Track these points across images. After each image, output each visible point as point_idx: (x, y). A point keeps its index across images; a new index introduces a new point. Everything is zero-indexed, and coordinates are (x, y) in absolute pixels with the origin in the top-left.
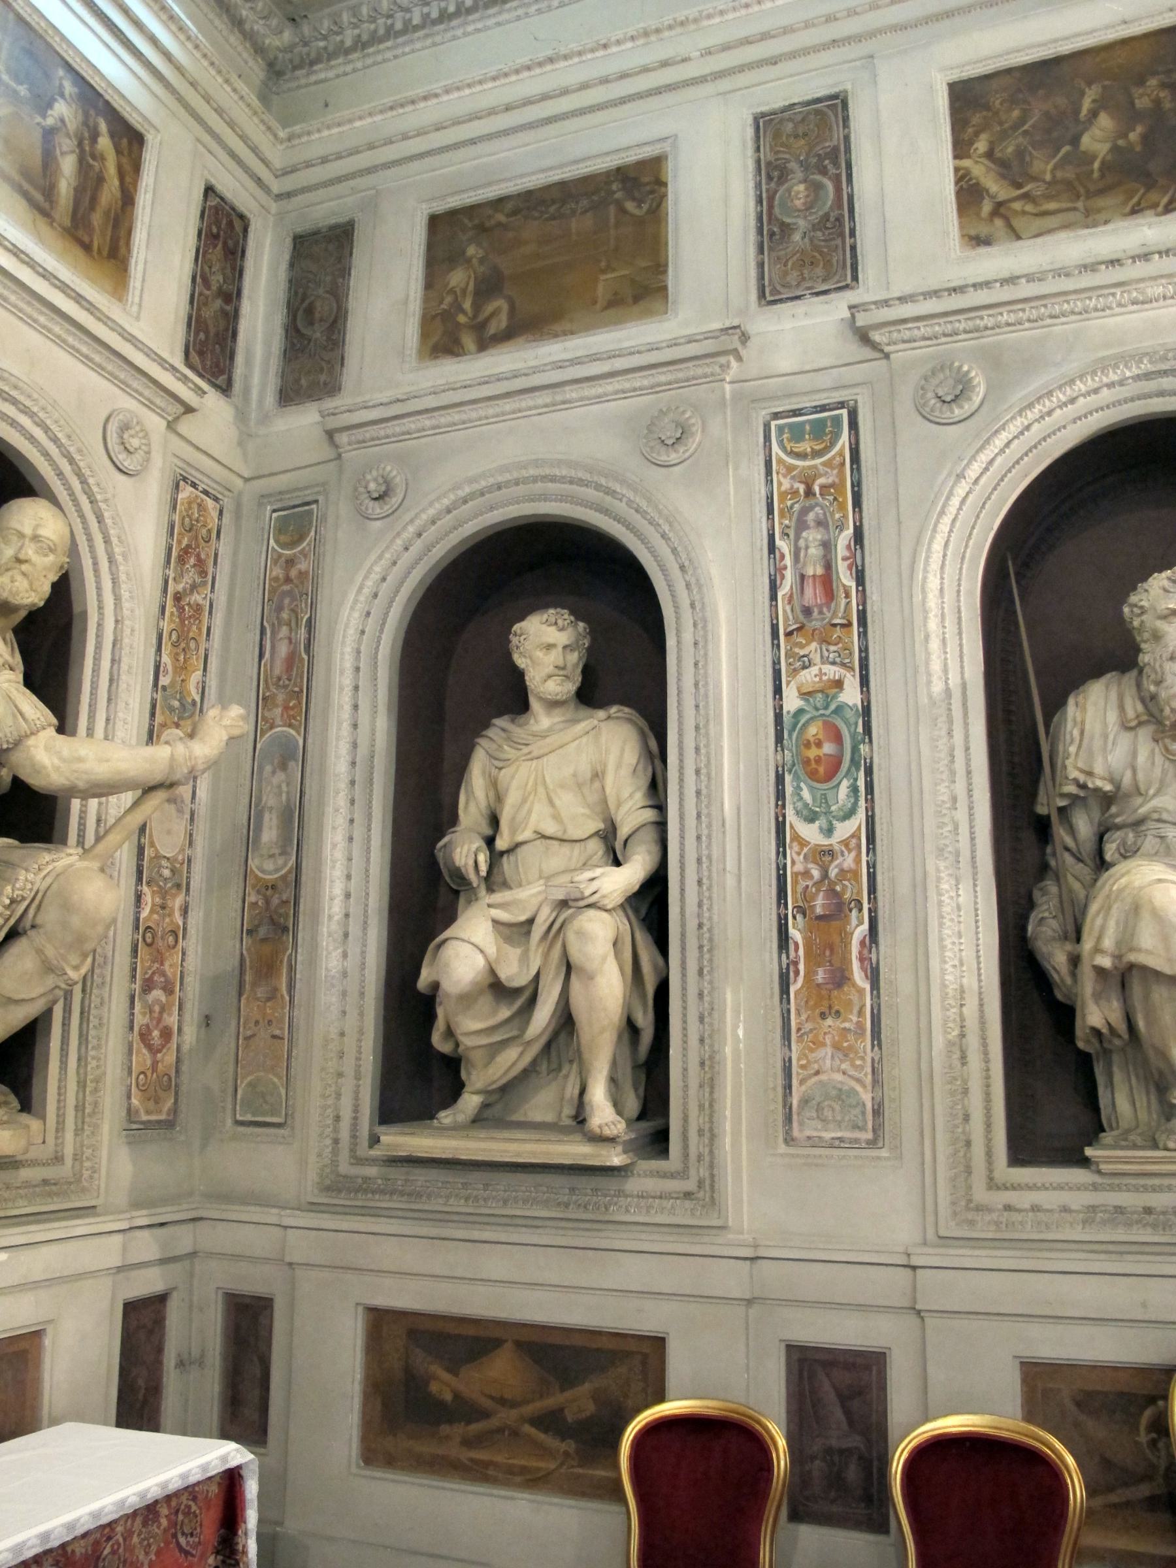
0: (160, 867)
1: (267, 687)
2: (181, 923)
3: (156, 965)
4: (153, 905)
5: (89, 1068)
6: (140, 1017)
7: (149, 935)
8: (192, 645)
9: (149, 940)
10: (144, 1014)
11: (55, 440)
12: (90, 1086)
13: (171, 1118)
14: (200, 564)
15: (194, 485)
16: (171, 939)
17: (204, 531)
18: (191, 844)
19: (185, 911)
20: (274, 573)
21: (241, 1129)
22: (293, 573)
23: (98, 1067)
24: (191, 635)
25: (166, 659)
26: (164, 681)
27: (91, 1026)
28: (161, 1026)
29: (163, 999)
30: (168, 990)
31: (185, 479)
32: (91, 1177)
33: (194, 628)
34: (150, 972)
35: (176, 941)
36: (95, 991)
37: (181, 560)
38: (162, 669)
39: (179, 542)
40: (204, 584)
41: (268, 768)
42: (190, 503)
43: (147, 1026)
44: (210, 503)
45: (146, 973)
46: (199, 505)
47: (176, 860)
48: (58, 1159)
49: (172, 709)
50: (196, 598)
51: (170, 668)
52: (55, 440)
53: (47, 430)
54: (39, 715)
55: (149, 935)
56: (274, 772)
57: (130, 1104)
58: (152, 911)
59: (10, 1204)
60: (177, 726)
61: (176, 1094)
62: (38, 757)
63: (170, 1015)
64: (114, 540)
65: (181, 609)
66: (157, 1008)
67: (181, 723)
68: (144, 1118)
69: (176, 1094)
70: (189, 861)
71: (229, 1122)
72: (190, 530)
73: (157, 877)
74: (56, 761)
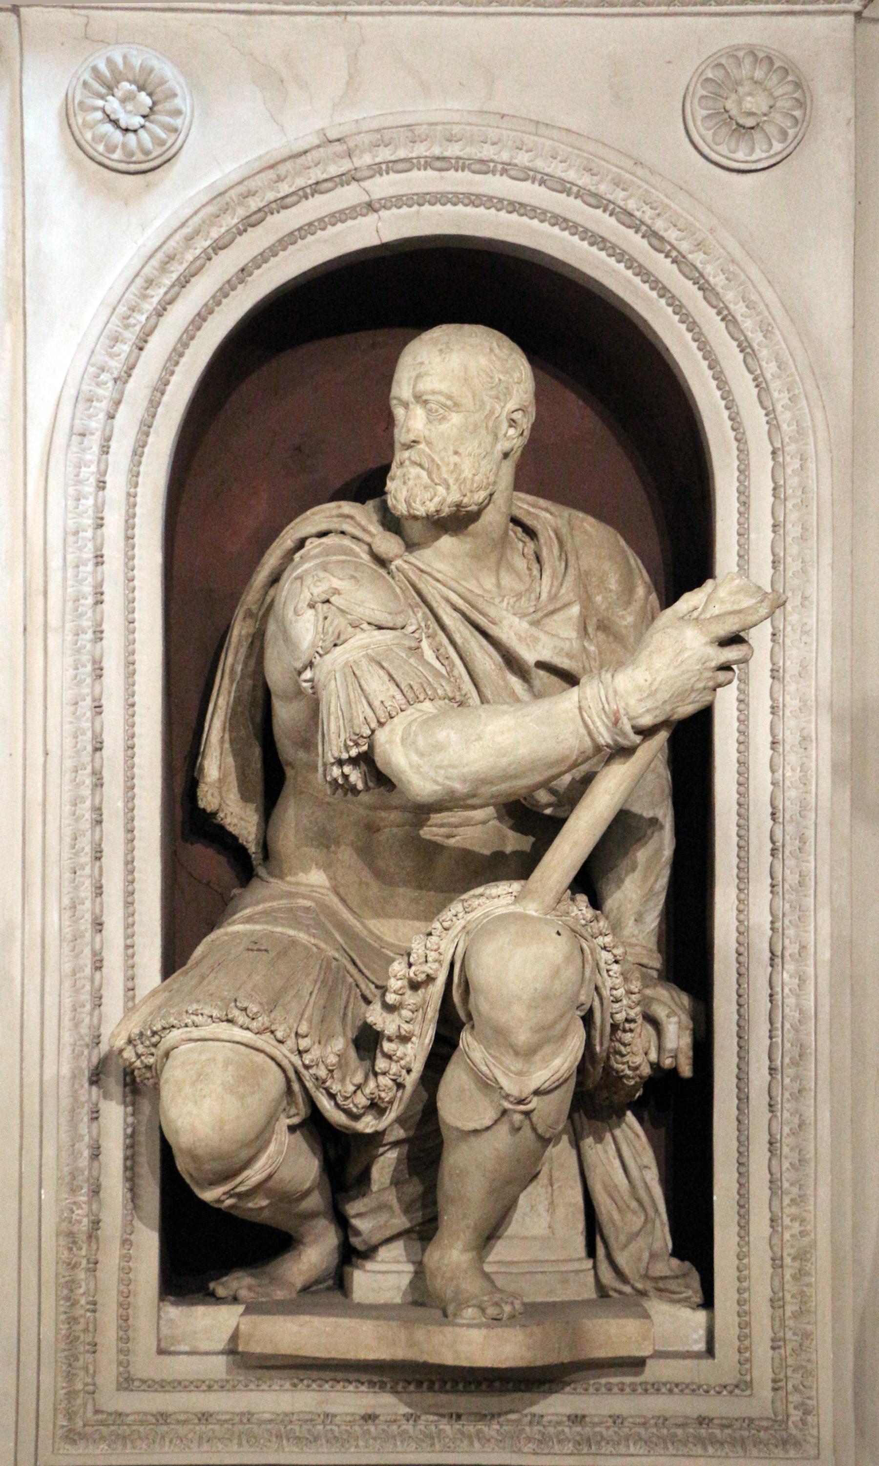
5: (787, 1236)
11: (564, 187)
23: (802, 1234)
32: (803, 1422)
36: (787, 1105)
52: (564, 187)
74: (415, 758)
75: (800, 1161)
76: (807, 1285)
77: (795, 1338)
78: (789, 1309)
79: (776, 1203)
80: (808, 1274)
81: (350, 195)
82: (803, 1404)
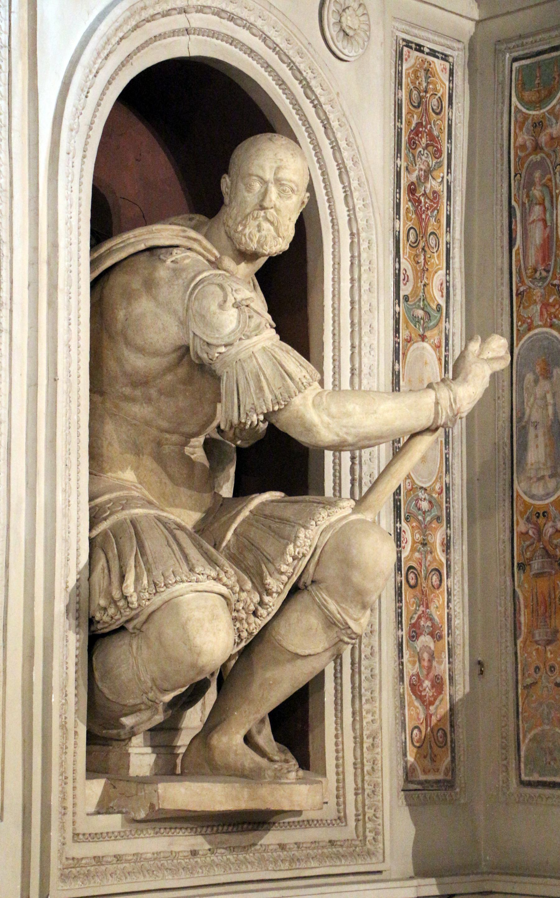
0: (418, 499)
1: (521, 281)
2: (444, 561)
3: (422, 608)
4: (414, 542)
6: (410, 666)
7: (411, 576)
8: (432, 241)
9: (412, 582)
10: (414, 664)
12: (367, 743)
13: (449, 778)
14: (433, 140)
15: (419, 48)
16: (435, 578)
17: (434, 102)
18: (447, 470)
19: (447, 546)
20: (520, 140)
21: (528, 791)
22: (543, 139)
24: (430, 230)
25: (405, 264)
26: (405, 290)
27: (363, 677)
28: (431, 675)
29: (432, 646)
30: (436, 636)
31: (408, 44)
33: (432, 220)
34: (416, 616)
35: (441, 581)
37: (412, 144)
38: (402, 277)
39: (409, 123)
40: (439, 165)
41: (530, 377)
42: (415, 72)
43: (418, 675)
44: (438, 64)
45: (412, 618)
46: (427, 71)
47: (434, 490)
48: (342, 819)
49: (416, 320)
50: (433, 184)
51: (410, 273)
52: (275, 48)
53: (265, 38)
54: (304, 373)
55: (411, 576)
56: (536, 381)
57: (406, 762)
58: (413, 550)
59: (303, 865)
60: (423, 338)
61: (453, 750)
62: (308, 416)
63: (440, 663)
64: (343, 144)
65: (416, 202)
66: (426, 656)
67: (428, 334)
68: (422, 777)
69: (453, 750)
70: (448, 489)
71: (514, 781)
72: (418, 107)
73: (414, 510)
74: (326, 419)
75: (372, 676)
76: (377, 754)
77: (370, 787)
78: (367, 768)
79: (357, 702)
80: (378, 747)
81: (179, 21)
82: (375, 828)
